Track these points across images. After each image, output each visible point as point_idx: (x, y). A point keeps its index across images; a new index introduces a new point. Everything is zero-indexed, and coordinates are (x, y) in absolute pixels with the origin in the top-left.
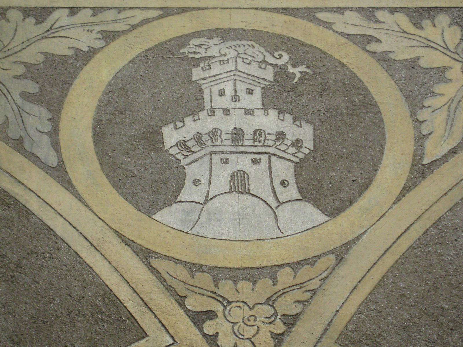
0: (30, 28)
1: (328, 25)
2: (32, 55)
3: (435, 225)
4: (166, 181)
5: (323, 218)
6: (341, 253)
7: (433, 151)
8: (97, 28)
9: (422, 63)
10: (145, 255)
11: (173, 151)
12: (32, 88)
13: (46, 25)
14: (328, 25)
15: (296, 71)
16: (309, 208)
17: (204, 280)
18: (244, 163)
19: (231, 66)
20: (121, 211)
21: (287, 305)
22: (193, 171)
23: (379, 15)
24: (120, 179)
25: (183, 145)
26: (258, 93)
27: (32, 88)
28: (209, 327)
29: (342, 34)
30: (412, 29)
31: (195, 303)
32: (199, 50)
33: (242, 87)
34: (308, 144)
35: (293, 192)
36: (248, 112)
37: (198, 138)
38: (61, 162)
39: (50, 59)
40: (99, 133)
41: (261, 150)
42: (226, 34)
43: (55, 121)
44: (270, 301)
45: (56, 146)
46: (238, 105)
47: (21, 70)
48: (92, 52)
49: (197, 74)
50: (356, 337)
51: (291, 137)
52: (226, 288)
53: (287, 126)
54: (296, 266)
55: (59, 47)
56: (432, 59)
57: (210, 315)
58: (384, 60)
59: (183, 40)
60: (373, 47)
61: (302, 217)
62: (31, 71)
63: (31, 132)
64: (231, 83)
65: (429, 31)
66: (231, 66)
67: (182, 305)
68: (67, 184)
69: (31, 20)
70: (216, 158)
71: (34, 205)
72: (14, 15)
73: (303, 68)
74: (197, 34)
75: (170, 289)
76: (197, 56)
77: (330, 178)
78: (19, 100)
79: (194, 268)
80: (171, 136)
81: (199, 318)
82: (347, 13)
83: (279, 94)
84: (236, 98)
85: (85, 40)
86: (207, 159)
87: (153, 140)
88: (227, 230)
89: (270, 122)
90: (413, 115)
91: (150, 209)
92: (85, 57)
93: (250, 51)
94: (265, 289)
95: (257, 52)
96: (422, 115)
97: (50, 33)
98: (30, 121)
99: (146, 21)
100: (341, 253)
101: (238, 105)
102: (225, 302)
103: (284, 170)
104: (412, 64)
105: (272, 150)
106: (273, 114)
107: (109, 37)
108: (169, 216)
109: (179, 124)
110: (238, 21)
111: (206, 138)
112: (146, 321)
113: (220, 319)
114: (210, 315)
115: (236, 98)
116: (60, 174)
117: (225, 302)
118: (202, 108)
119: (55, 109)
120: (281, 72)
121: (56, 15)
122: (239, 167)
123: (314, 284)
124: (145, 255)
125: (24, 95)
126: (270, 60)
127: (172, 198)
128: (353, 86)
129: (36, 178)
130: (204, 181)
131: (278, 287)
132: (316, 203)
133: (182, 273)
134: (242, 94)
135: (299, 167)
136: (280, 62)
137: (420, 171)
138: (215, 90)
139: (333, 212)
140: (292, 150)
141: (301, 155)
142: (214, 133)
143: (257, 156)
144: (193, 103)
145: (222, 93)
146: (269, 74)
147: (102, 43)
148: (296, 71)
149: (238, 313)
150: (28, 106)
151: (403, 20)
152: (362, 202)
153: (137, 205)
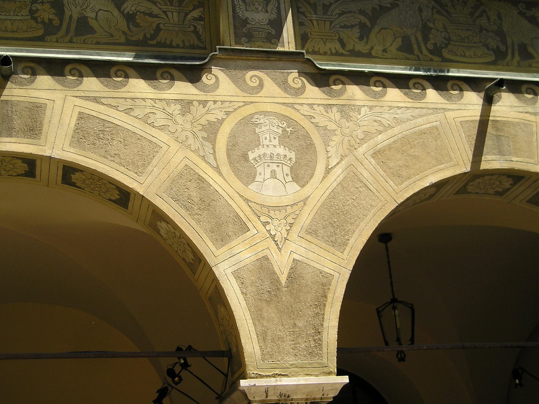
0: (203, 111)
1: (298, 111)
2: (203, 121)
3: (332, 191)
4: (251, 173)
5: (299, 188)
6: (305, 201)
7: (332, 164)
8: (224, 110)
9: (328, 128)
10: (247, 200)
11: (252, 162)
12: (205, 135)
13: (206, 108)
14: (298, 111)
15: (288, 130)
16: (295, 184)
17: (265, 210)
18: (274, 167)
19: (268, 128)
20: (238, 184)
21: (290, 220)
22: (259, 170)
23: (315, 107)
24: (237, 172)
25: (255, 159)
26: (277, 138)
27: (205, 135)
28: (268, 227)
29: (303, 115)
30: (325, 113)
31: (263, 219)
32: (257, 120)
33: (272, 136)
34: (294, 160)
35: (289, 179)
36: (275, 146)
37: (259, 156)
38: (218, 165)
39: (210, 123)
40: (229, 156)
41: (280, 162)
42: (265, 113)
43: (214, 148)
44: (285, 218)
45: (215, 159)
46: (271, 143)
47: (201, 127)
48: (223, 120)
49: (257, 130)
50: (310, 231)
51: (288, 157)
52: (272, 213)
53: (287, 152)
54: (292, 206)
55: (212, 118)
56: (332, 126)
57: (268, 223)
58: (316, 125)
59: (252, 115)
60: (313, 120)
61: (293, 187)
62: (204, 128)
63: (207, 153)
64: (268, 134)
65: (331, 115)
66: (268, 128)
67: (259, 220)
68: (220, 174)
69: (201, 106)
70: (266, 164)
71: (211, 182)
72: (195, 103)
73: (291, 129)
74: (256, 113)
75: (255, 214)
76: (257, 123)
77: (300, 174)
78: (202, 140)
79: (262, 205)
80: (251, 156)
81: (265, 224)
82: (304, 105)
83: (285, 139)
84: (270, 141)
85: (221, 115)
86: (263, 165)
87: (245, 157)
88: (270, 193)
89: (281, 150)
90: (326, 148)
91: (247, 184)
92: (221, 122)
93: (274, 121)
94: (283, 214)
95: (276, 121)
96: (329, 149)
97: (208, 112)
98: (206, 148)
99: (240, 107)
100: (305, 201)
101: (271, 143)
102: (272, 218)
103: (287, 170)
104: (325, 128)
105: (283, 162)
106: (282, 147)
107: (228, 113)
108: (253, 187)
109: (253, 151)
110: (269, 108)
111: (262, 156)
112: (249, 225)
113: (271, 224)
114: (268, 223)
115: (270, 141)
116: (217, 169)
117: (272, 218)
118: (260, 145)
119: (213, 142)
120: (284, 130)
121: (210, 103)
122: (273, 169)
123: (297, 212)
124: (247, 200)
125: (202, 137)
126: (281, 125)
127: (253, 181)
128: (307, 136)
129: (210, 172)
130: (263, 174)
131: (287, 214)
132: (297, 182)
133: (258, 207)
134: (272, 139)
135: (291, 168)
136: (283, 126)
137: (328, 171)
138: (264, 137)
139: (303, 186)
140: (289, 162)
141: (292, 164)
142: (264, 154)
143: (278, 164)
144: (257, 144)
145: (266, 139)
146: (280, 131)
147: (225, 117)
148: (288, 130)
149: (276, 222)
150: (205, 143)
151: (321, 108)
152: (311, 182)
153: (243, 183)
